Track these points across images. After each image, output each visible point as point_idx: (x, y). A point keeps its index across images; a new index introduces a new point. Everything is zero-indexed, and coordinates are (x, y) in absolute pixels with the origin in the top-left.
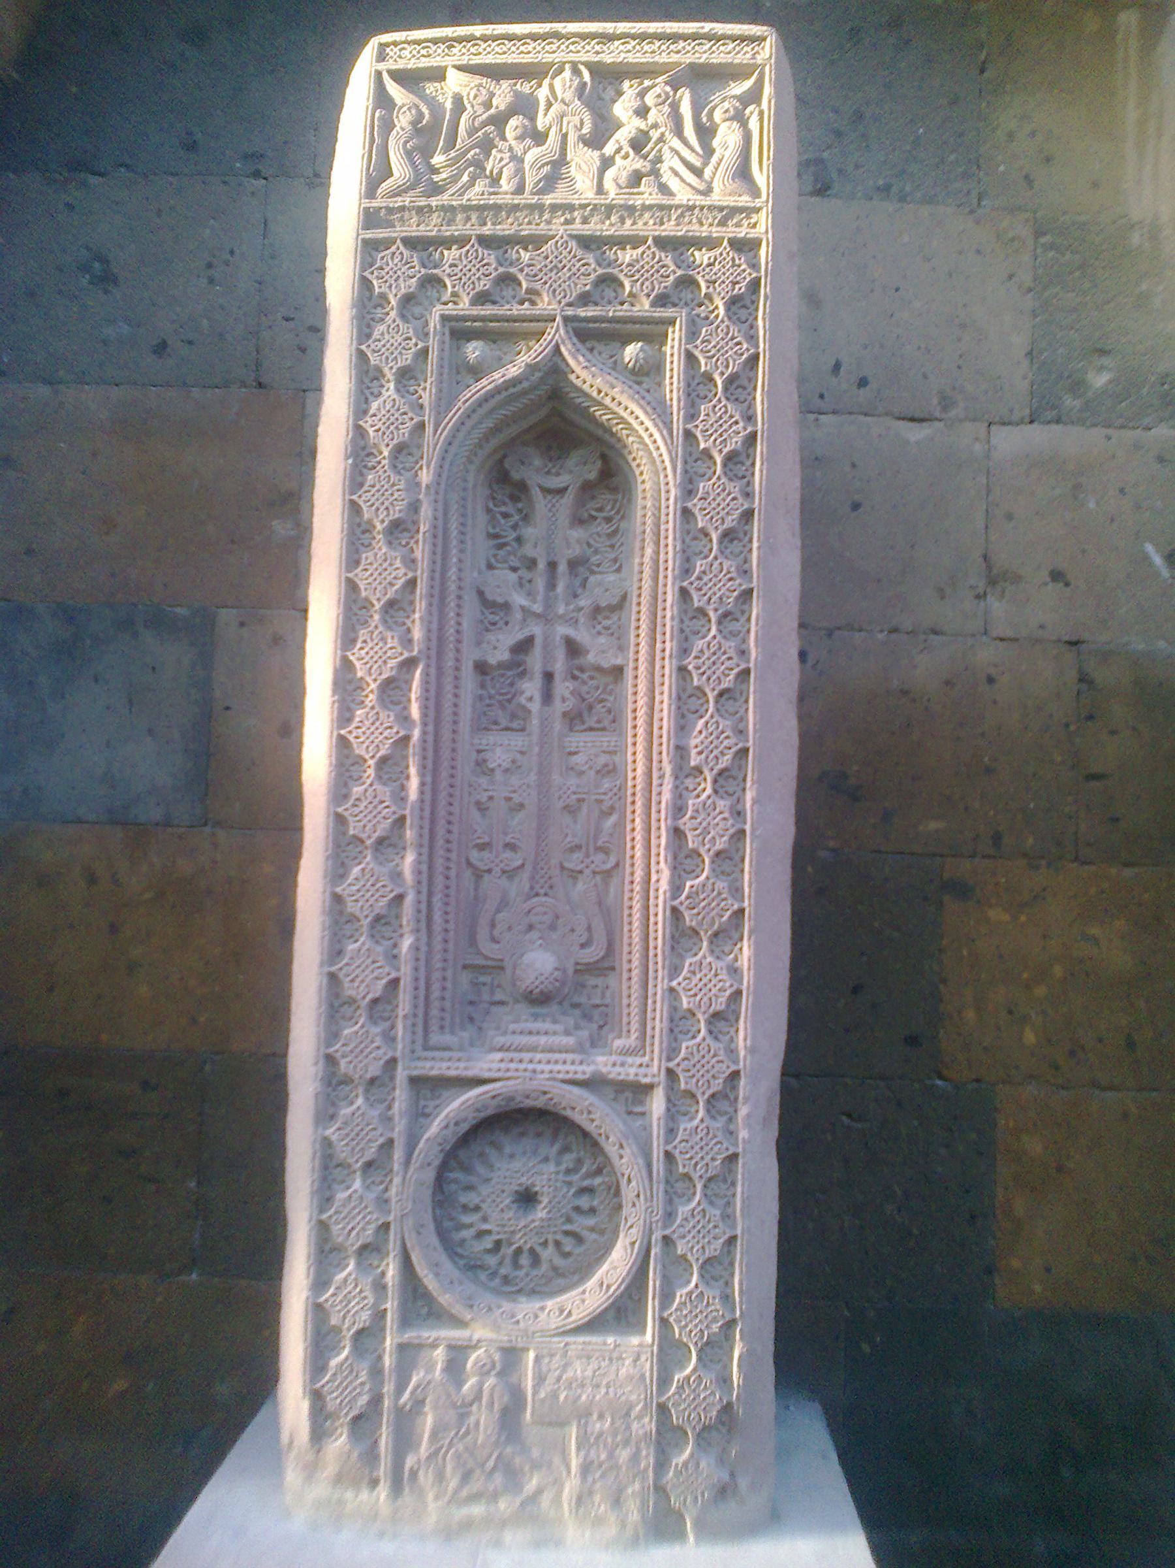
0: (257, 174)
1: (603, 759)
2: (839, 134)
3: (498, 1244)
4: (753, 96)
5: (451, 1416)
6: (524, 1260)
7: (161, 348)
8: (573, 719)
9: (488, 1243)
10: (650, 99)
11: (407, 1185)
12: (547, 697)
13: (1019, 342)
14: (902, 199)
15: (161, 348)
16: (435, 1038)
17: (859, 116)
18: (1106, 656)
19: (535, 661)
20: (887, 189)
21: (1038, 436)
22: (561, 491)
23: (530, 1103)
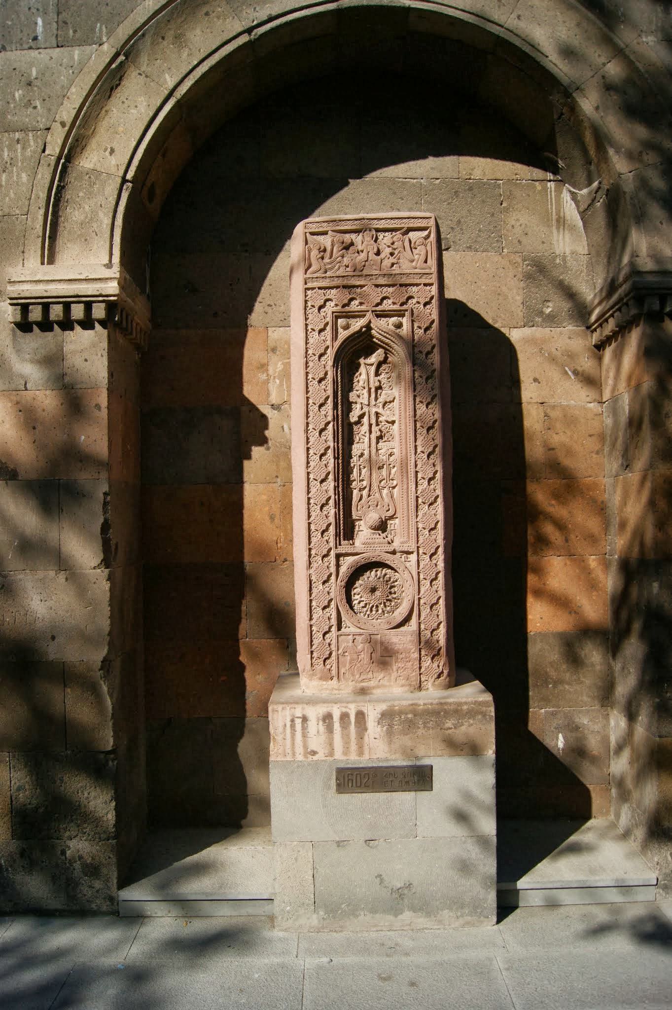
0: (246, 251)
1: (390, 451)
2: (452, 228)
3: (366, 604)
4: (428, 236)
5: (355, 656)
6: (374, 609)
7: (215, 315)
8: (379, 438)
9: (362, 604)
10: (395, 239)
11: (335, 588)
12: (370, 432)
13: (519, 298)
14: (476, 251)
15: (215, 315)
16: (342, 542)
17: (459, 222)
18: (553, 407)
19: (365, 420)
20: (470, 247)
21: (527, 331)
22: (372, 365)
23: (374, 560)
